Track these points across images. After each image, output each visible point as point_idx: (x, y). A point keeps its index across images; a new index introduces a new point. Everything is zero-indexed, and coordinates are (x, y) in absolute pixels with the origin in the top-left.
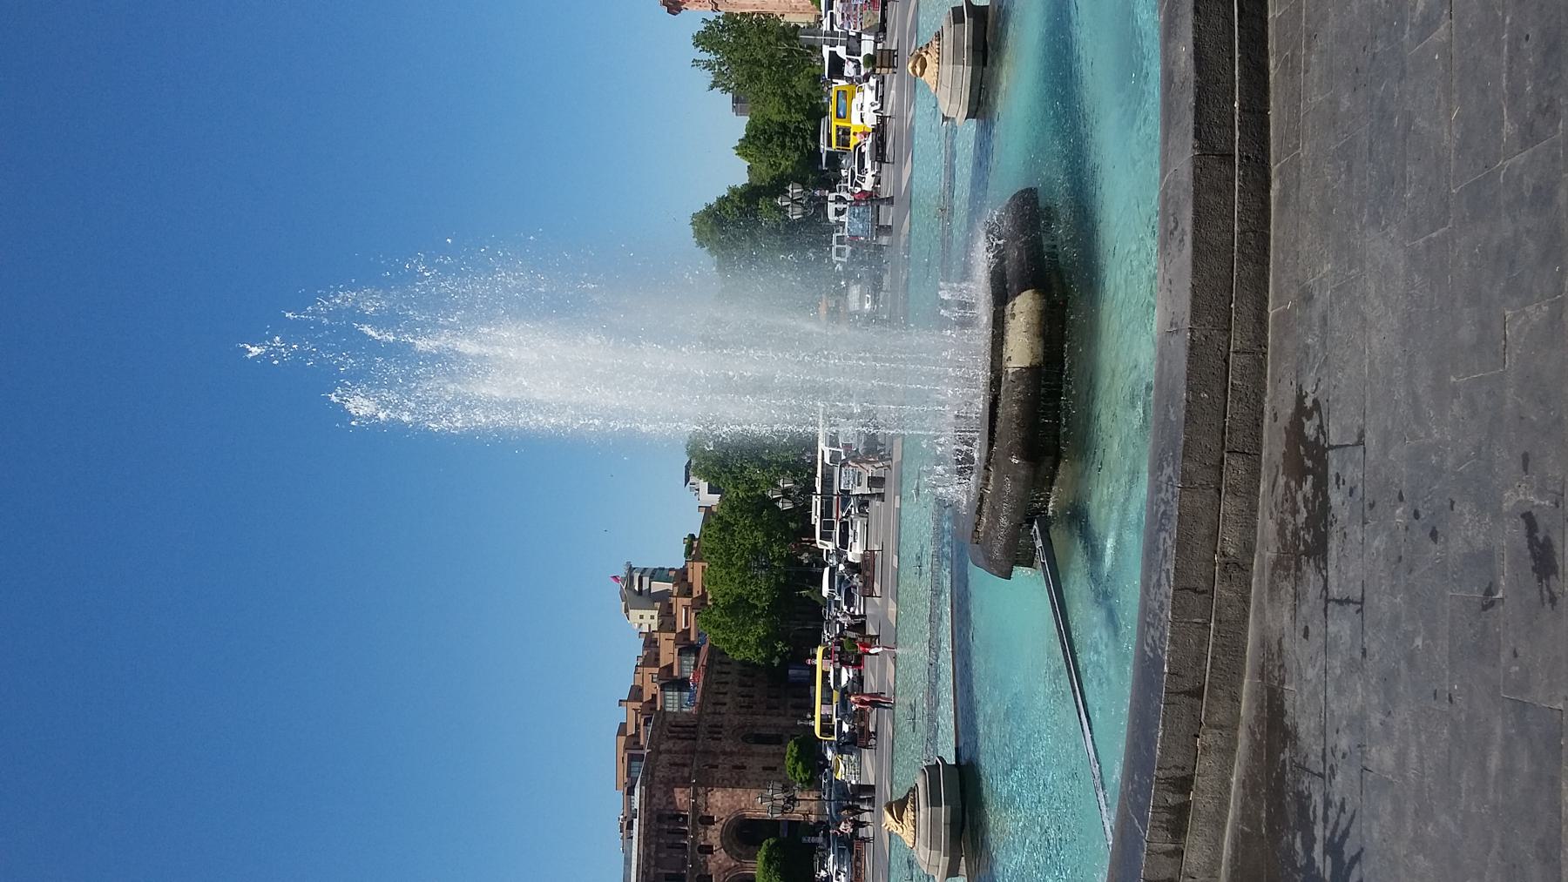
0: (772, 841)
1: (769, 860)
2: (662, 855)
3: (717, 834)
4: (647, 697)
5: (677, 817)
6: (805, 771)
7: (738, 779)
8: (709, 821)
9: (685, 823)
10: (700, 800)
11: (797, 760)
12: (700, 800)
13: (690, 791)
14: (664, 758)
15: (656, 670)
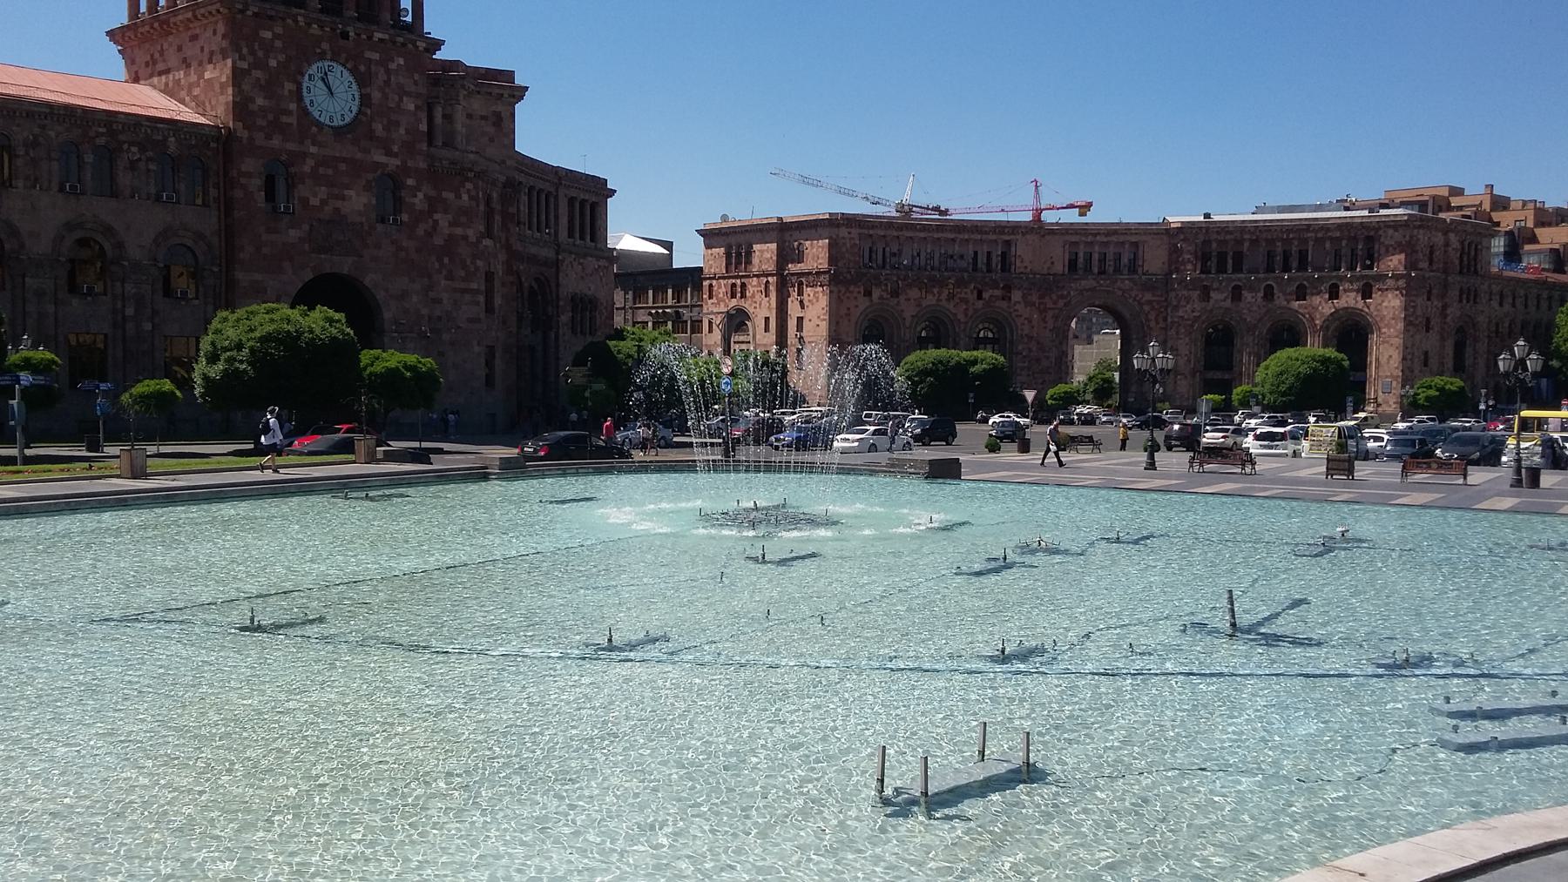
0: (1346, 363)
1: (1325, 361)
2: (1328, 245)
3: (1352, 303)
4: (1496, 216)
5: (1371, 258)
6: (1428, 398)
7: (1415, 323)
8: (1366, 293)
9: (1365, 267)
10: (1390, 283)
11: (1441, 390)
12: (1390, 283)
13: (1401, 270)
14: (1439, 239)
15: (1530, 224)
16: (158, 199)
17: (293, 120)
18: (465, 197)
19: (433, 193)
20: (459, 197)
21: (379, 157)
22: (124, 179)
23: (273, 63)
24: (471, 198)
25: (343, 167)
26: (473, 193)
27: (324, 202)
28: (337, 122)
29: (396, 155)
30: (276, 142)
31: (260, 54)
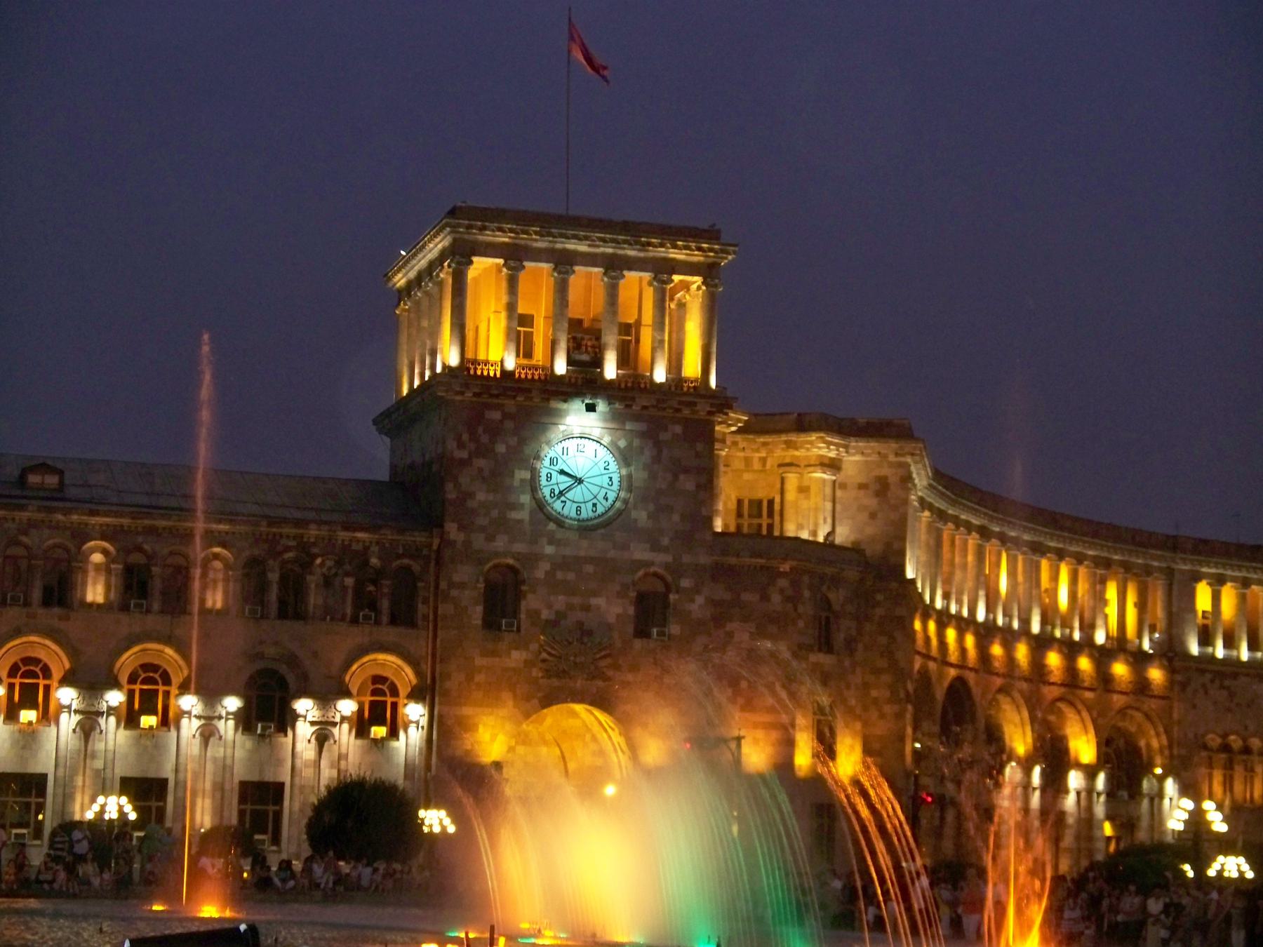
16: (355, 621)
17: (523, 515)
18: (776, 598)
19: (727, 596)
20: (765, 598)
21: (640, 553)
22: (314, 599)
23: (501, 448)
24: (788, 599)
25: (589, 569)
26: (789, 592)
27: (560, 616)
28: (587, 512)
29: (666, 550)
30: (500, 543)
31: (485, 439)
